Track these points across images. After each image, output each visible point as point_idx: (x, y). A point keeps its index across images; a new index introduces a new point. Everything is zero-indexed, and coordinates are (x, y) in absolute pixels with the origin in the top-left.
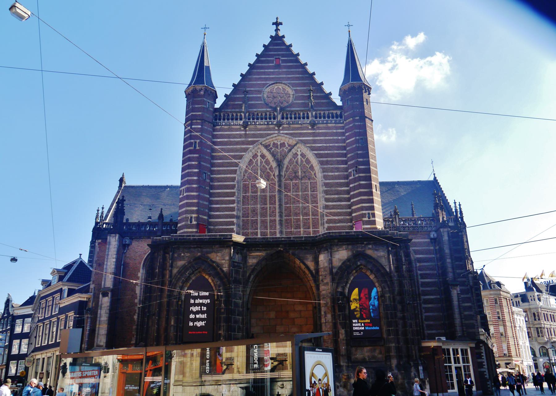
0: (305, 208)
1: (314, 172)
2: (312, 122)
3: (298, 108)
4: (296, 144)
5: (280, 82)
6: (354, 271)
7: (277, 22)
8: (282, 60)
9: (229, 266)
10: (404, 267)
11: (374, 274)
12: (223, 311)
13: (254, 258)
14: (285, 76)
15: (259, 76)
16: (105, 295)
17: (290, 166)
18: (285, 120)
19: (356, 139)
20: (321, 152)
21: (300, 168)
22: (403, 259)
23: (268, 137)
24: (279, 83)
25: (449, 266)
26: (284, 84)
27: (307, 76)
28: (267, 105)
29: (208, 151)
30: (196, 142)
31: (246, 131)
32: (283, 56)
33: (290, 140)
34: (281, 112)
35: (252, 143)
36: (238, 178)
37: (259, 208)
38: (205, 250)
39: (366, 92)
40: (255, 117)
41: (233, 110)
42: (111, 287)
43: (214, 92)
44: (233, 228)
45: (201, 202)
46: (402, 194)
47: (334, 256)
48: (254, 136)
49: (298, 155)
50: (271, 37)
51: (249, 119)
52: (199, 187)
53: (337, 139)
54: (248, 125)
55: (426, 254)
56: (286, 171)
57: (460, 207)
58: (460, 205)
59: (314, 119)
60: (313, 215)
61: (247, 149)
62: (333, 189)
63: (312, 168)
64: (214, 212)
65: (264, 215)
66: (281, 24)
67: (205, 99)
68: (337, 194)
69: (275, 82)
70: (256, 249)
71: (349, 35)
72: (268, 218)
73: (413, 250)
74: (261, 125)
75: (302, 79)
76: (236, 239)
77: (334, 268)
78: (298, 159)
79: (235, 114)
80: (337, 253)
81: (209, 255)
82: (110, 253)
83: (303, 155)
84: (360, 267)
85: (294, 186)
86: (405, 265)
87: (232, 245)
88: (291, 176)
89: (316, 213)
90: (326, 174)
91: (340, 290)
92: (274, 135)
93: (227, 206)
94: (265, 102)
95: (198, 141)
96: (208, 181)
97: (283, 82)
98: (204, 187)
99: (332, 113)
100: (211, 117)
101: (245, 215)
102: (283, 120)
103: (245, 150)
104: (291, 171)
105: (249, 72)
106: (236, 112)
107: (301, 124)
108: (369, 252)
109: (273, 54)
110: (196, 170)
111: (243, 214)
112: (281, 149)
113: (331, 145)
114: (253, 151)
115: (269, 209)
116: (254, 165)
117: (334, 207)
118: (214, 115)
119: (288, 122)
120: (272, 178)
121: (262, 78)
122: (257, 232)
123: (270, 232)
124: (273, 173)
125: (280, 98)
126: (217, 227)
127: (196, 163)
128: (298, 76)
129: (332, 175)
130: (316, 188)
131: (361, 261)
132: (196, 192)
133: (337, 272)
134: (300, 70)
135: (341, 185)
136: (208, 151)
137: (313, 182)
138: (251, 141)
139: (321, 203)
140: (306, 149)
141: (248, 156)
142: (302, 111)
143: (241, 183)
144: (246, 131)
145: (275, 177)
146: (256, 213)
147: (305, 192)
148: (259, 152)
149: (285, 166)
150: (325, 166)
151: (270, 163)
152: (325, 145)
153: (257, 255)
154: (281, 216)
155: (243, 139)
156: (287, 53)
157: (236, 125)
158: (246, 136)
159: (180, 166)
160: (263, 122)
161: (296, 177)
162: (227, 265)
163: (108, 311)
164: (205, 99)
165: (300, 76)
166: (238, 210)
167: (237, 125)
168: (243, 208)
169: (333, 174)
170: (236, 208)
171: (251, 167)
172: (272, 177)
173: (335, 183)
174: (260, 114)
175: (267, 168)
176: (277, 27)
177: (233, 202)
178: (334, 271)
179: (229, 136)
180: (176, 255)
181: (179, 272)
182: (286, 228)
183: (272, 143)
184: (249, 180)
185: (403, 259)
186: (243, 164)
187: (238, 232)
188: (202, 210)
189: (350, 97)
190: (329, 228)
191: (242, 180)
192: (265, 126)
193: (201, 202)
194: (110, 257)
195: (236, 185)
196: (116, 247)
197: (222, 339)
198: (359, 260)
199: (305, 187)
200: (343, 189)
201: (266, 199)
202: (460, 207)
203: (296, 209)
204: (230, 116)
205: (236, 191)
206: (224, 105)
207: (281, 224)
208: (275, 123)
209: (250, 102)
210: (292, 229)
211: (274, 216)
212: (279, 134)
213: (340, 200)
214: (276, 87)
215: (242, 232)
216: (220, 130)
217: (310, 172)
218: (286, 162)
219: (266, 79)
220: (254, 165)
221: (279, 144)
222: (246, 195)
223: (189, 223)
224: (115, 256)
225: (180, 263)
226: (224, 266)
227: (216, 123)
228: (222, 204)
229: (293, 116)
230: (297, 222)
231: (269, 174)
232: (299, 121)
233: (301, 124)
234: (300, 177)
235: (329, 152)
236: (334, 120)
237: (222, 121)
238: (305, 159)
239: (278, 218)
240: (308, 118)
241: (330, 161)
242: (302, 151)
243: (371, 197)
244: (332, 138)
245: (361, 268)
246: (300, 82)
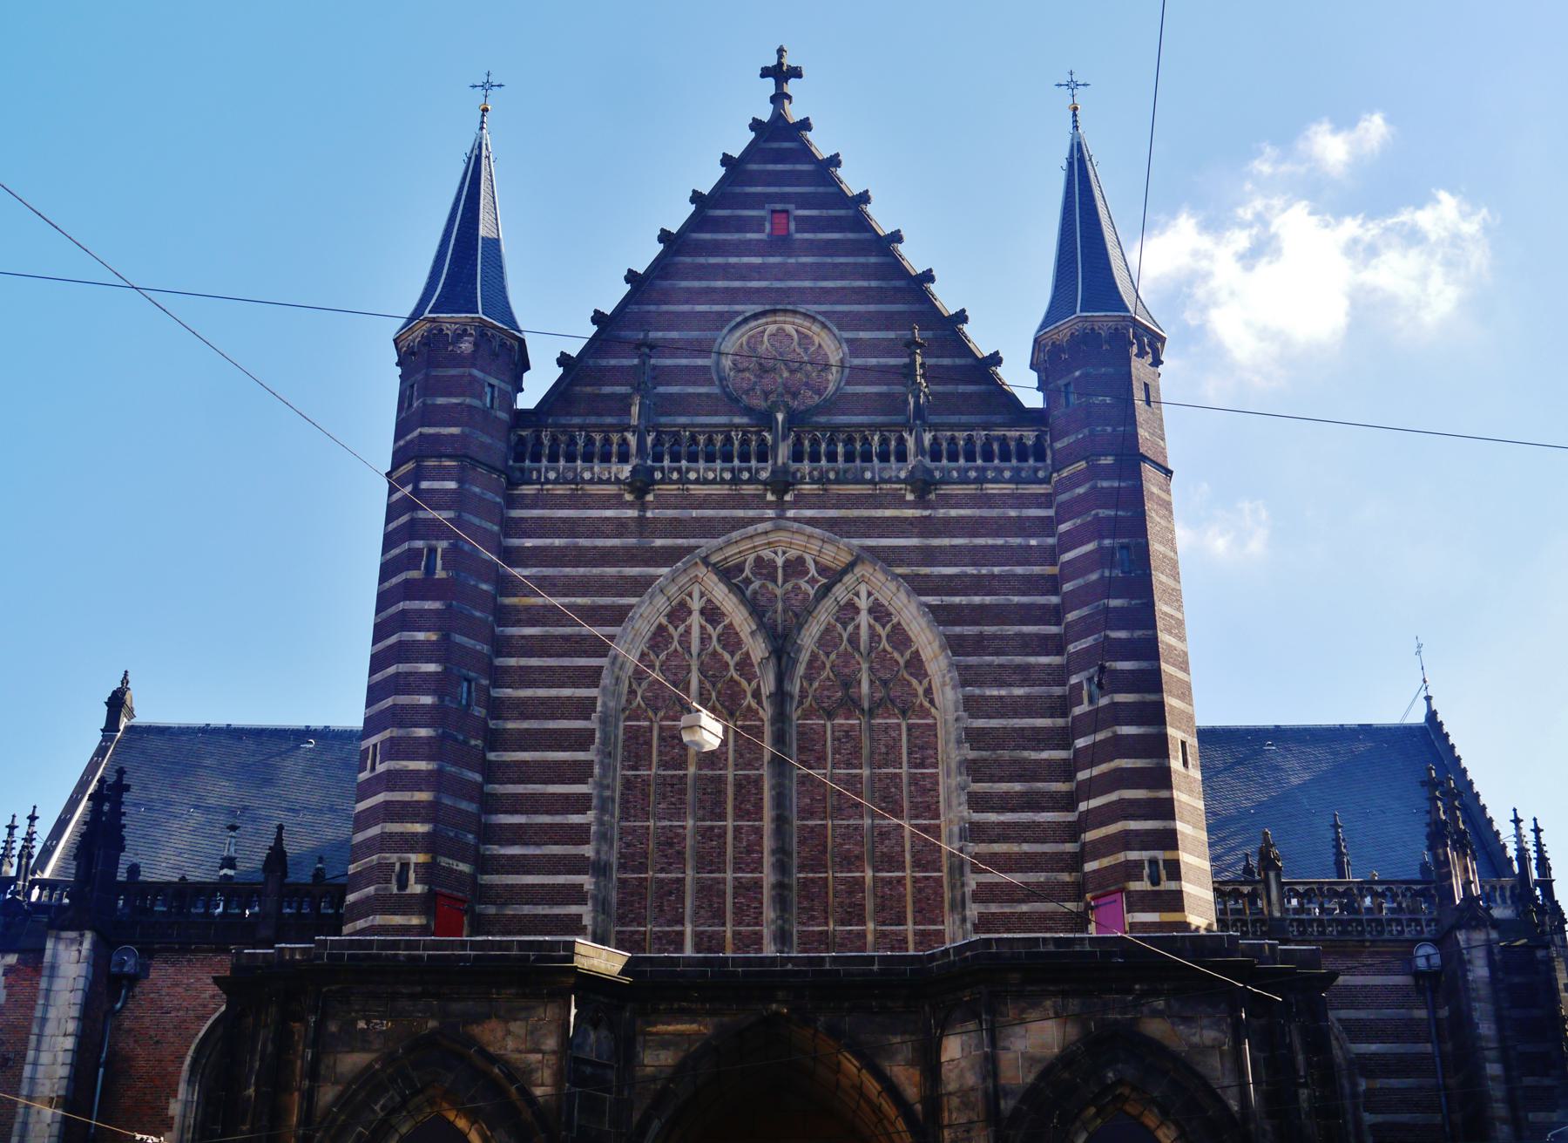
0: (884, 835)
1: (925, 682)
2: (919, 475)
3: (862, 414)
4: (850, 567)
6: (1092, 1110)
7: (780, 64)
8: (797, 218)
9: (558, 1081)
10: (1304, 1093)
11: (1177, 1124)
14: (808, 284)
15: (704, 284)
17: (823, 657)
18: (806, 466)
19: (1100, 549)
20: (957, 600)
21: (865, 666)
22: (1300, 1058)
23: (735, 535)
24: (785, 311)
25: (1497, 1091)
26: (806, 316)
27: (898, 283)
28: (731, 401)
29: (484, 587)
30: (432, 551)
31: (644, 507)
32: (804, 201)
33: (826, 546)
34: (790, 429)
35: (669, 557)
36: (604, 704)
38: (455, 1007)
39: (1141, 354)
40: (683, 450)
41: (593, 420)
43: (516, 344)
44: (580, 917)
46: (1295, 781)
47: (1007, 1044)
48: (676, 527)
49: (857, 611)
50: (756, 125)
51: (658, 458)
52: (442, 738)
53: (1020, 546)
54: (655, 482)
55: (1397, 1038)
56: (809, 677)
57: (1538, 838)
58: (1537, 831)
59: (927, 461)
60: (917, 865)
61: (648, 581)
62: (1006, 754)
63: (916, 665)
64: (501, 843)
65: (711, 863)
66: (796, 73)
67: (476, 372)
69: (768, 307)
70: (676, 1006)
71: (1075, 121)
72: (729, 875)
73: (1339, 1020)
74: (706, 482)
75: (879, 296)
76: (595, 962)
77: (1006, 1095)
78: (858, 627)
79: (598, 437)
80: (1019, 1030)
81: (476, 1030)
82: (52, 1014)
83: (879, 612)
84: (1118, 1092)
85: (839, 740)
86: (1305, 1085)
87: (574, 989)
88: (829, 697)
89: (929, 858)
90: (977, 691)
92: (761, 527)
93: (558, 819)
94: (724, 388)
95: (442, 545)
96: (479, 712)
97: (802, 308)
98: (461, 738)
99: (1003, 441)
100: (501, 445)
102: (797, 465)
103: (640, 586)
104: (828, 678)
106: (606, 430)
107: (872, 482)
108: (1156, 1028)
109: (764, 194)
110: (432, 667)
111: (622, 856)
112: (789, 586)
113: (996, 570)
114: (672, 590)
115: (735, 838)
116: (672, 649)
118: (513, 438)
119: (821, 472)
120: (749, 706)
121: (714, 290)
122: (682, 934)
123: (735, 934)
124: (754, 684)
125: (786, 374)
126: (509, 911)
127: (433, 637)
128: (864, 284)
129: (1001, 697)
130: (931, 752)
131: (1120, 1066)
132: (429, 758)
134: (873, 260)
135: (1039, 739)
136: (484, 587)
137: (919, 725)
138: (662, 547)
139: (954, 813)
140: (892, 586)
141: (648, 613)
142: (874, 427)
143: (616, 727)
144: (644, 507)
145: (760, 703)
146: (678, 853)
147: (886, 766)
148: (696, 595)
149: (805, 657)
151: (739, 643)
152: (970, 570)
153: (681, 1034)
154: (782, 867)
155: (632, 541)
156: (821, 189)
157: (601, 481)
158: (643, 526)
159: (363, 648)
160: (714, 471)
161: (850, 704)
162: (547, 1075)
164: (476, 372)
165: (874, 284)
166: (604, 837)
167: (608, 482)
168: (623, 831)
169: (1003, 692)
170: (593, 829)
171: (663, 656)
172: (749, 700)
173: (1014, 729)
174: (702, 439)
175: (727, 665)
176: (779, 86)
177: (581, 803)
178: (1007, 1105)
179: (570, 528)
180: (333, 1028)
181: (342, 1101)
182: (805, 917)
183: (751, 558)
184: (650, 714)
185: (1300, 1058)
186: (628, 647)
187: (599, 931)
188: (452, 834)
189: (1077, 374)
190: (984, 923)
191: (624, 710)
192: (723, 490)
193: (447, 801)
194: (50, 1028)
195: (597, 735)
196: (81, 986)
199: (887, 746)
200: (1045, 755)
201: (721, 792)
202: (1538, 838)
203: (847, 837)
204: (581, 443)
205: (596, 759)
206: (557, 396)
207: (782, 902)
208: (764, 475)
209: (661, 389)
210: (827, 924)
211: (752, 866)
212: (783, 523)
214: (772, 328)
215: (618, 933)
216: (537, 501)
217: (909, 684)
218: (809, 637)
219: (731, 296)
220: (672, 649)
221: (780, 561)
222: (636, 776)
223: (395, 891)
224: (71, 1026)
225: (352, 1062)
227: (522, 470)
228: (535, 813)
229: (840, 449)
230: (850, 893)
231: (736, 689)
232: (863, 471)
233: (872, 482)
234: (866, 705)
235: (988, 599)
236: (1012, 469)
237: (545, 462)
238: (888, 627)
239: (768, 877)
240: (902, 457)
241: (994, 637)
242: (876, 595)
243: (1163, 794)
244: (1000, 541)
245: (1121, 1094)
246: (872, 308)
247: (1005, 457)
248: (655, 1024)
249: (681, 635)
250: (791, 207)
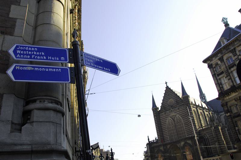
28: (169, 106)
32: (169, 91)
63: (181, 119)
83: (179, 117)
103: (166, 119)
108: (188, 142)
135: (188, 122)
158: (166, 116)
190: (187, 134)
213: (188, 126)
219: (167, 99)
225: (156, 151)
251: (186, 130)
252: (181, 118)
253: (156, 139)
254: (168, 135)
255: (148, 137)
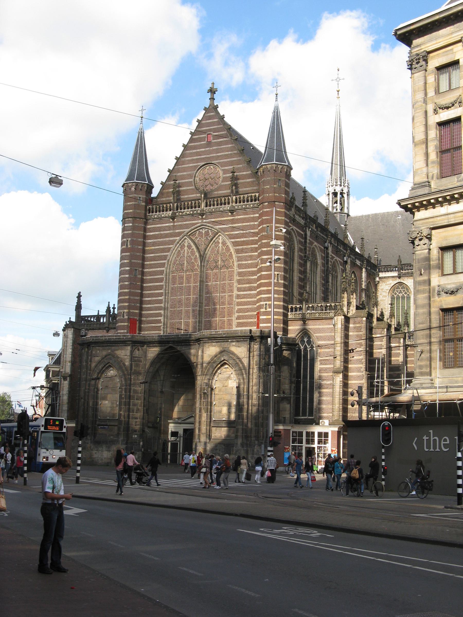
5: (210, 162)
12: (123, 396)
13: (152, 353)
14: (214, 155)
16: (65, 379)
18: (208, 207)
20: (238, 240)
29: (140, 247)
31: (174, 223)
32: (215, 130)
35: (178, 234)
37: (183, 299)
42: (70, 373)
45: (132, 298)
48: (181, 227)
51: (177, 210)
52: (131, 283)
53: (253, 225)
59: (234, 204)
63: (231, 255)
68: (248, 283)
69: (205, 163)
81: (116, 352)
83: (224, 243)
90: (241, 263)
91: (206, 381)
93: (157, 298)
95: (130, 239)
99: (251, 196)
101: (173, 306)
103: (172, 242)
105: (183, 155)
110: (128, 268)
117: (245, 296)
122: (182, 321)
125: (210, 180)
127: (128, 261)
128: (227, 153)
130: (233, 277)
133: (206, 367)
134: (230, 146)
135: (253, 273)
136: (140, 247)
144: (174, 223)
147: (223, 281)
150: (240, 255)
155: (172, 231)
156: (219, 126)
158: (174, 227)
161: (216, 267)
163: (68, 392)
165: (229, 153)
169: (246, 263)
173: (248, 271)
177: (161, 295)
178: (204, 365)
179: (160, 229)
181: (96, 366)
190: (238, 318)
197: (122, 417)
198: (223, 356)
201: (190, 289)
206: (161, 193)
208: (199, 211)
218: (208, 252)
219: (198, 161)
224: (71, 347)
225: (97, 359)
226: (126, 361)
229: (216, 203)
232: (220, 208)
235: (245, 239)
241: (246, 248)
244: (248, 224)
246: (229, 160)
247: (252, 201)
248: (150, 349)
249: (183, 252)
250: (212, 132)
251: (239, 304)
252: (232, 250)
253: (108, 310)
254: (160, 308)
255: (79, 296)
